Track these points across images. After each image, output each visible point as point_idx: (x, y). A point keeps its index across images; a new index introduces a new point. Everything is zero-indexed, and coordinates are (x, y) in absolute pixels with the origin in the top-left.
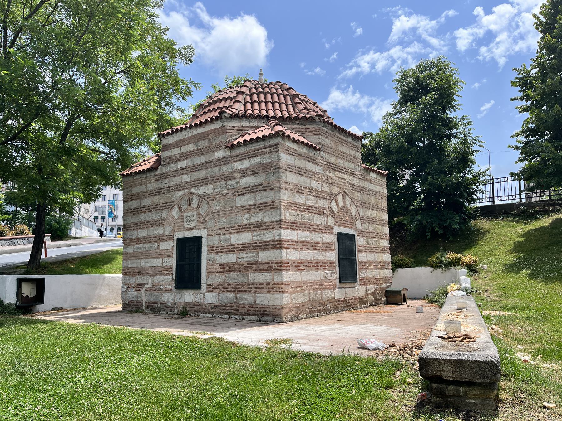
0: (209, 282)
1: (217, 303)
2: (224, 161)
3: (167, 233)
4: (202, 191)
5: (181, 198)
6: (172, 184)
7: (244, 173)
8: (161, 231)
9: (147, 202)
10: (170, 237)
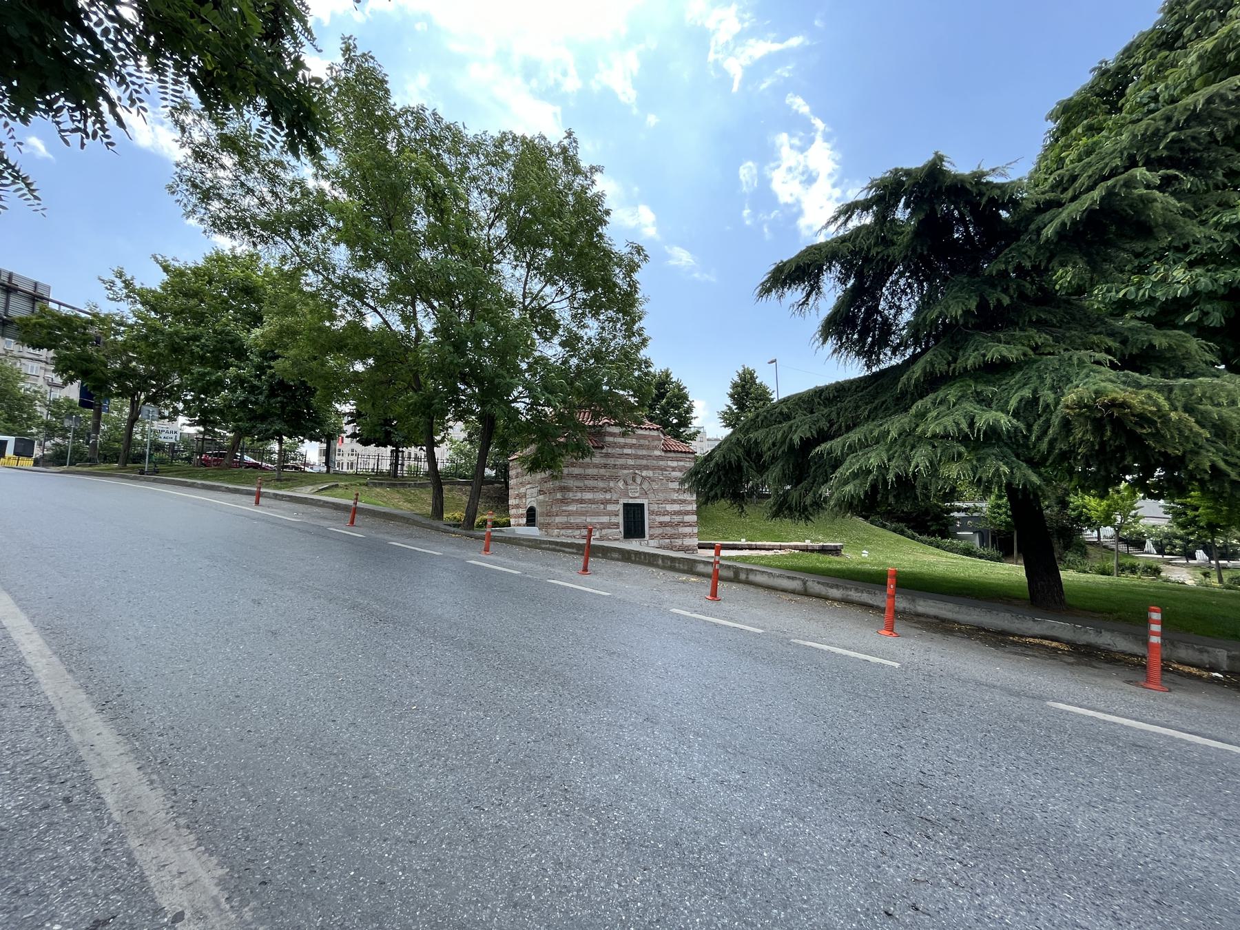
2: (659, 458)
4: (644, 473)
5: (627, 475)
7: (674, 469)
8: (608, 496)
9: (590, 471)
10: (617, 502)
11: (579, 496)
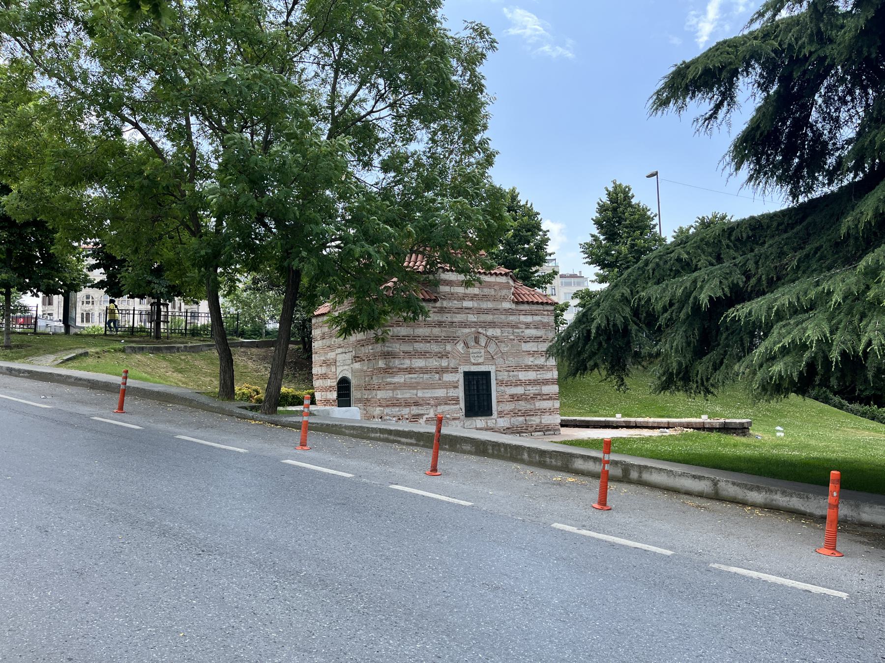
0: (500, 409)
1: (508, 426)
2: (508, 312)
3: (452, 365)
4: (490, 332)
5: (469, 334)
6: (455, 320)
7: (528, 326)
8: (444, 363)
10: (455, 370)
11: (407, 363)
